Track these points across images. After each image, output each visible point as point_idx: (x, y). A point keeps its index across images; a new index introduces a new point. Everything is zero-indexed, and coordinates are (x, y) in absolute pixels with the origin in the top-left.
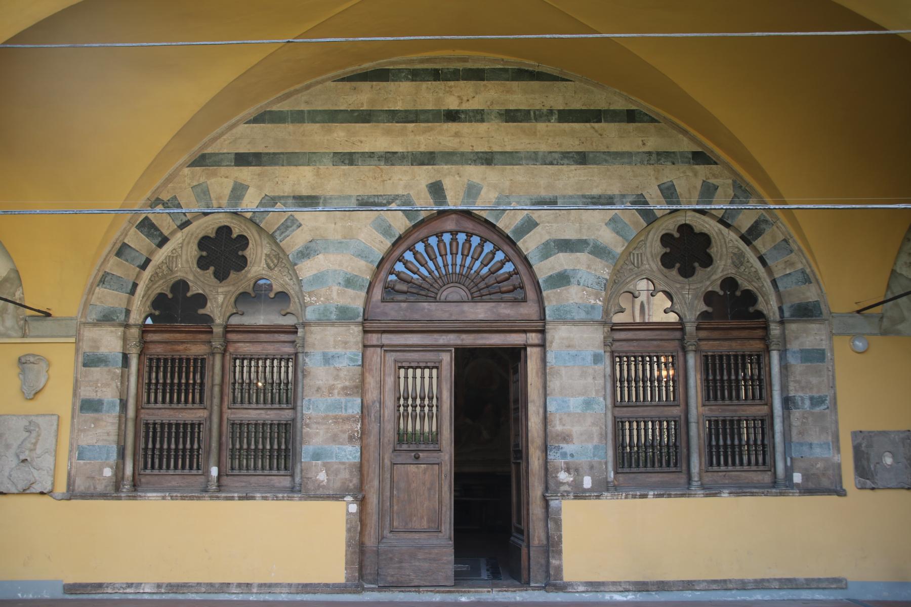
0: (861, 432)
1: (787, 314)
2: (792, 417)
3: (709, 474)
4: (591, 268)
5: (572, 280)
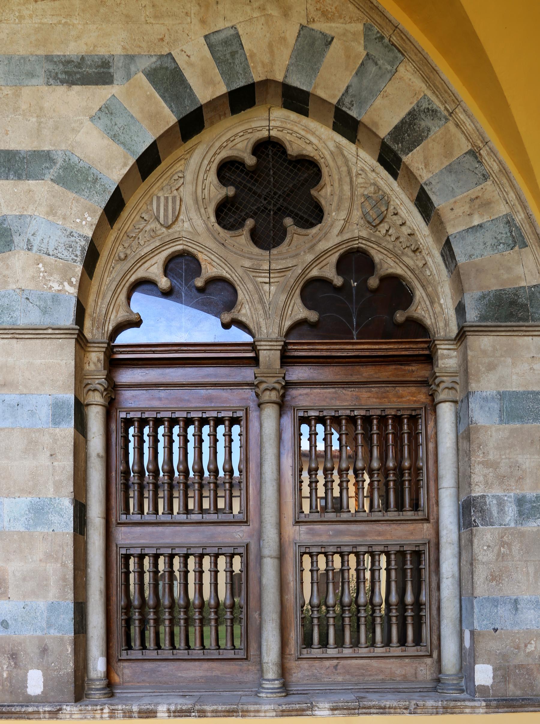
1: (472, 315)
2: (476, 541)
3: (305, 664)
4: (55, 215)
5: (16, 239)
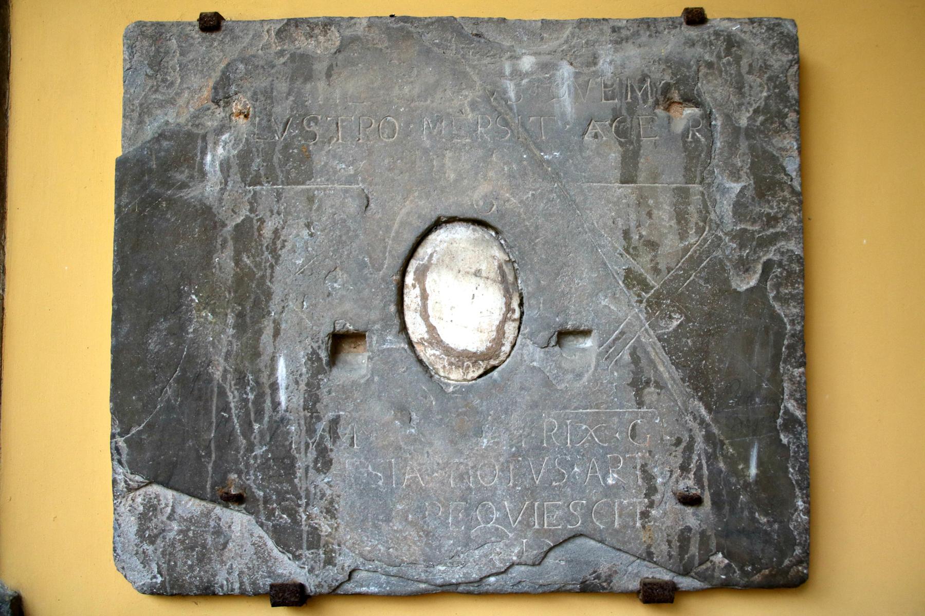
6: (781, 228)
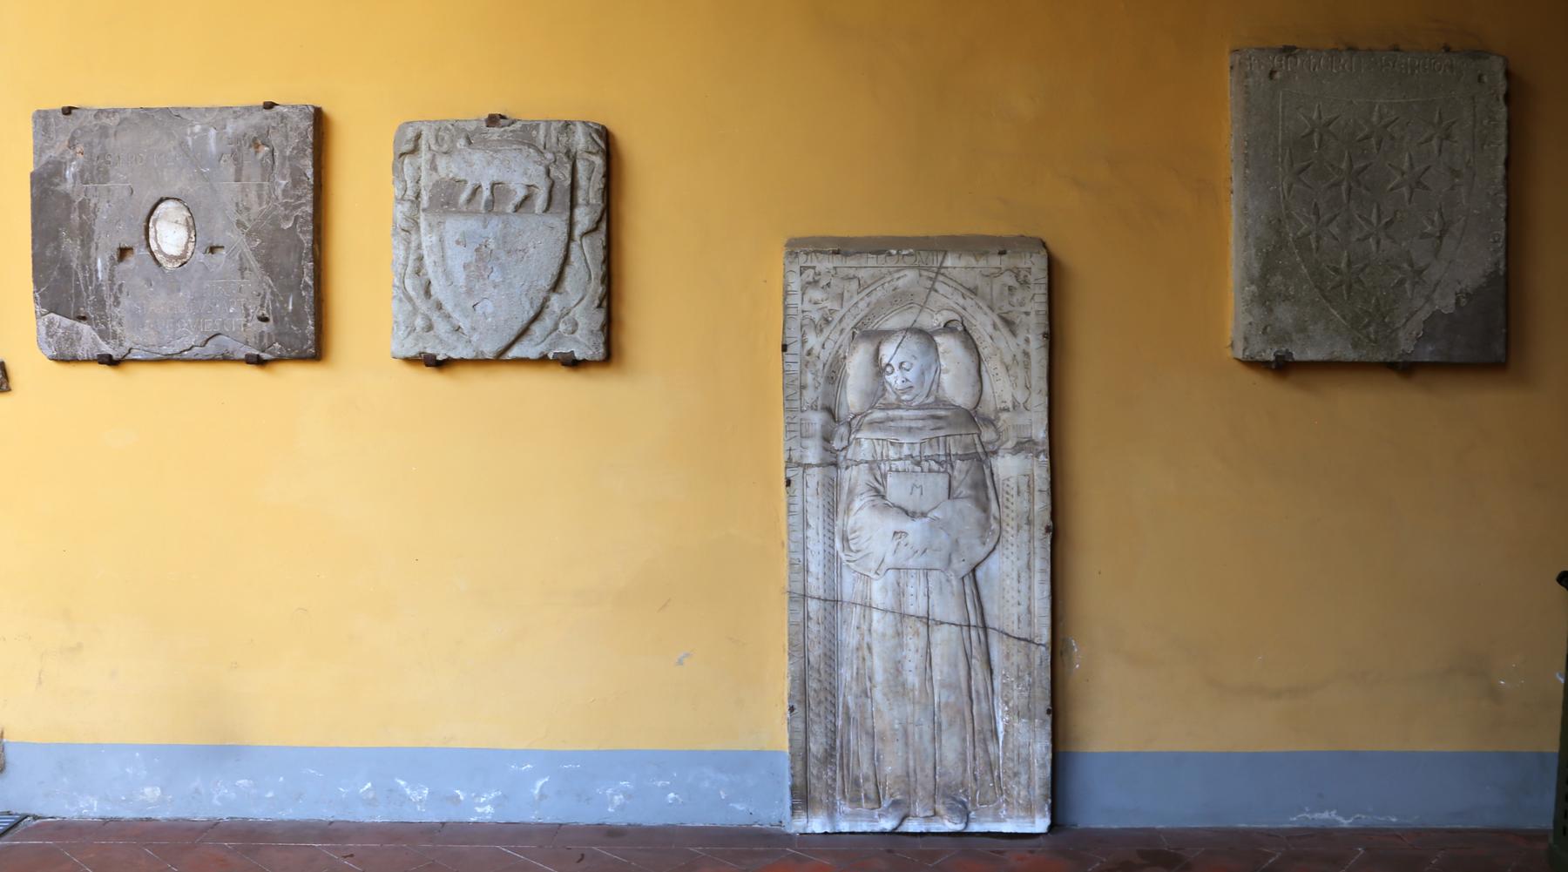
0: (68, 111)
6: (303, 201)
